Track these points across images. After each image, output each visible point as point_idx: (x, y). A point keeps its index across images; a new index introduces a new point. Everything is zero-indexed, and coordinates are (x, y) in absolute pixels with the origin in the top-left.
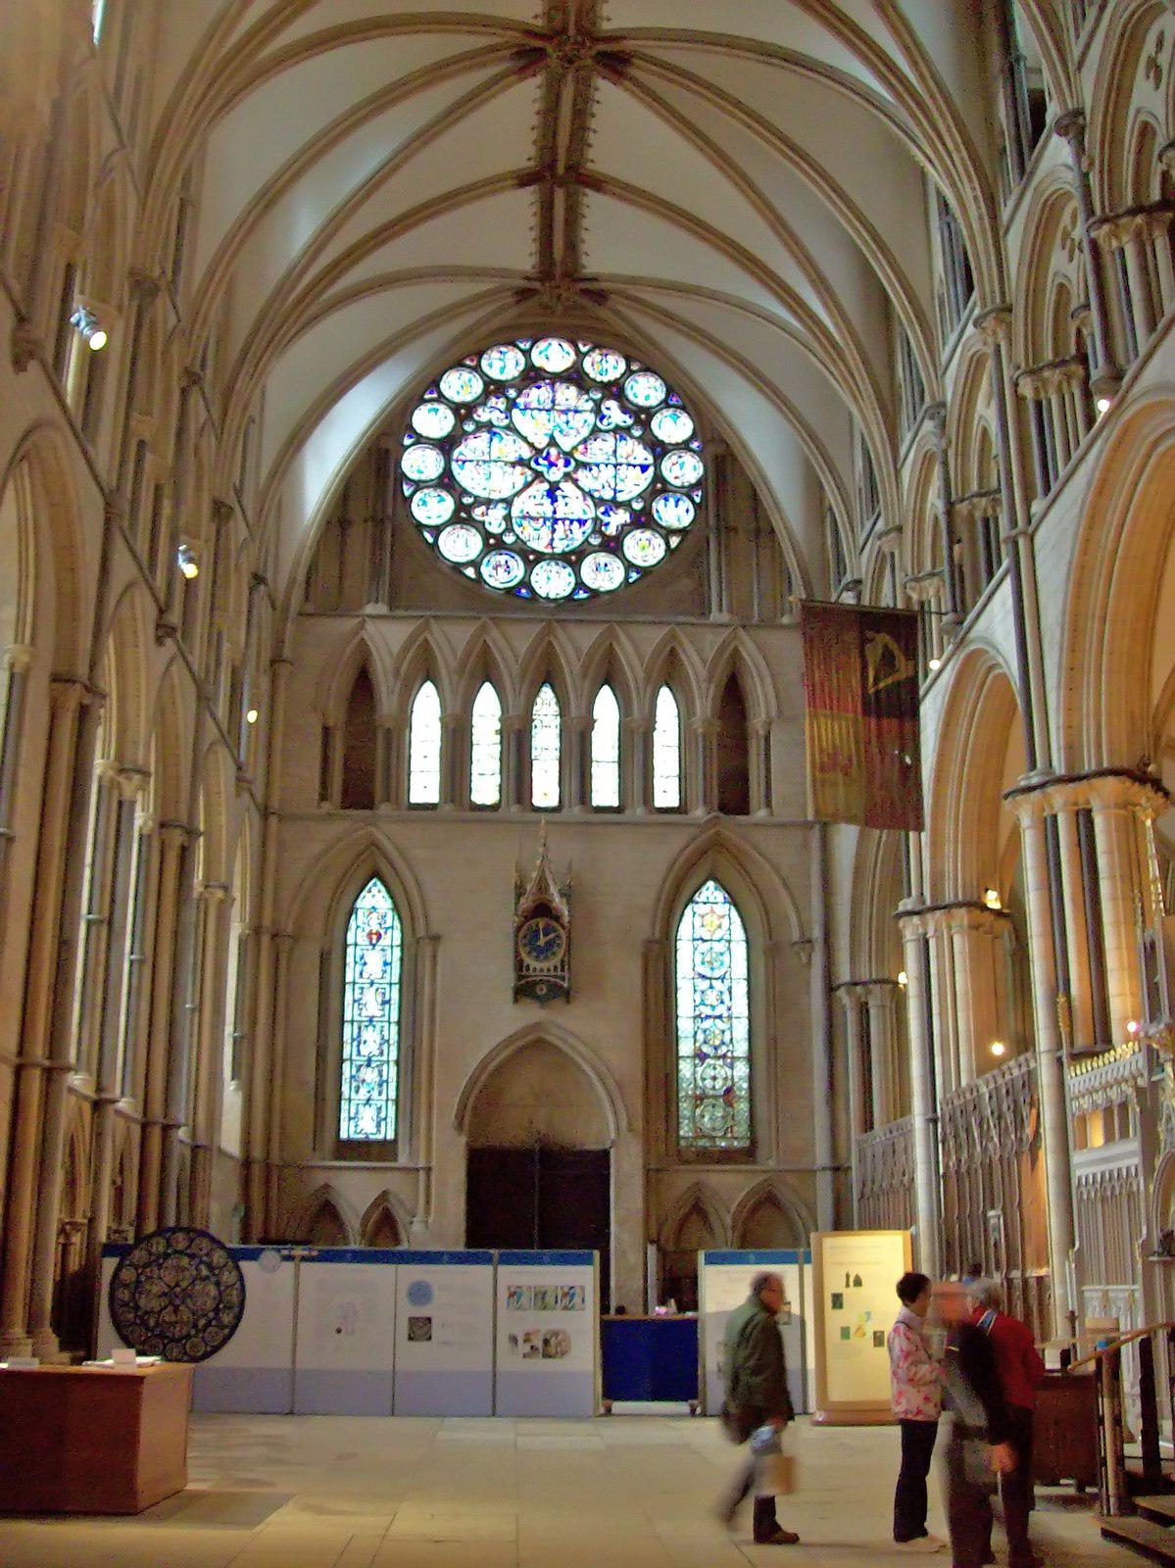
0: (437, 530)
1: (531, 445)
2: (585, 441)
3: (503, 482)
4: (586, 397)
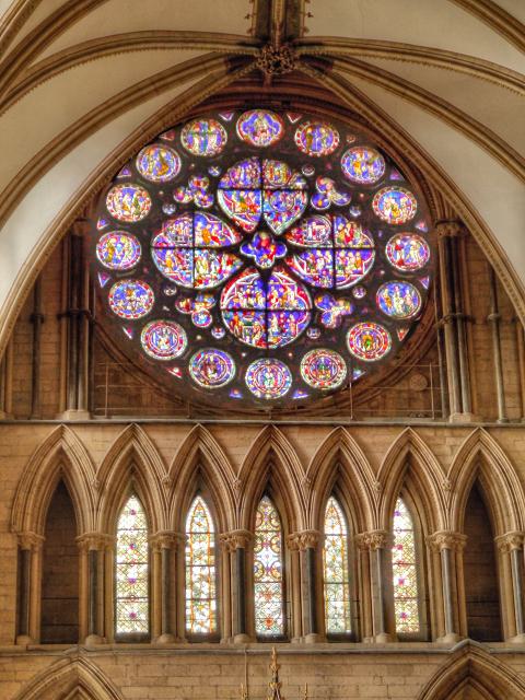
0: (137, 326)
1: (239, 230)
2: (297, 224)
3: (209, 270)
4: (298, 175)
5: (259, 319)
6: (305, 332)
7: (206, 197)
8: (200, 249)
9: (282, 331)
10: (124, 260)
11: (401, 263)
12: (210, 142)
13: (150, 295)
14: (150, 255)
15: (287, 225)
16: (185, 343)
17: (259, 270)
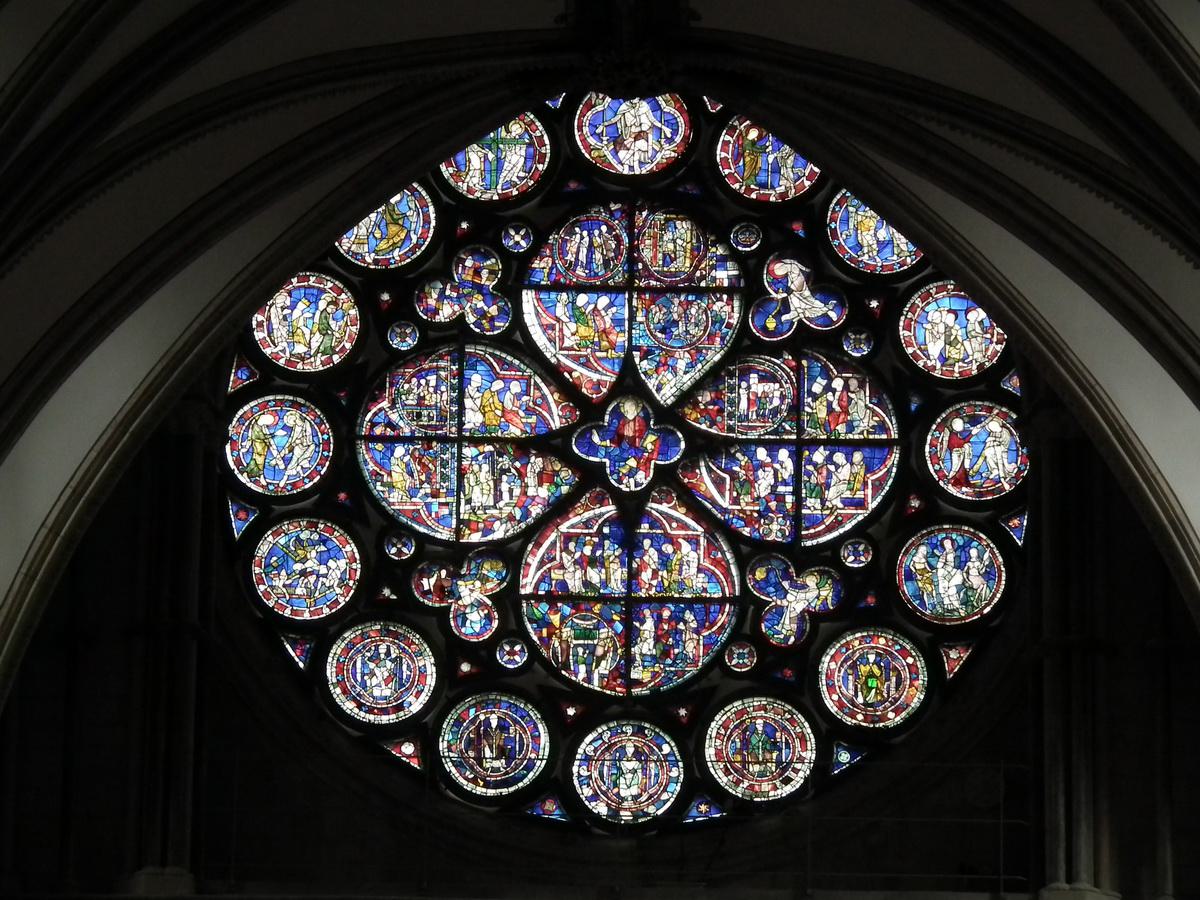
0: (321, 635)
1: (569, 391)
2: (713, 378)
4: (720, 251)
5: (611, 622)
7: (493, 310)
8: (475, 441)
9: (666, 653)
10: (292, 471)
11: (962, 479)
14: (354, 453)
15: (687, 381)
16: (431, 681)
17: (619, 497)
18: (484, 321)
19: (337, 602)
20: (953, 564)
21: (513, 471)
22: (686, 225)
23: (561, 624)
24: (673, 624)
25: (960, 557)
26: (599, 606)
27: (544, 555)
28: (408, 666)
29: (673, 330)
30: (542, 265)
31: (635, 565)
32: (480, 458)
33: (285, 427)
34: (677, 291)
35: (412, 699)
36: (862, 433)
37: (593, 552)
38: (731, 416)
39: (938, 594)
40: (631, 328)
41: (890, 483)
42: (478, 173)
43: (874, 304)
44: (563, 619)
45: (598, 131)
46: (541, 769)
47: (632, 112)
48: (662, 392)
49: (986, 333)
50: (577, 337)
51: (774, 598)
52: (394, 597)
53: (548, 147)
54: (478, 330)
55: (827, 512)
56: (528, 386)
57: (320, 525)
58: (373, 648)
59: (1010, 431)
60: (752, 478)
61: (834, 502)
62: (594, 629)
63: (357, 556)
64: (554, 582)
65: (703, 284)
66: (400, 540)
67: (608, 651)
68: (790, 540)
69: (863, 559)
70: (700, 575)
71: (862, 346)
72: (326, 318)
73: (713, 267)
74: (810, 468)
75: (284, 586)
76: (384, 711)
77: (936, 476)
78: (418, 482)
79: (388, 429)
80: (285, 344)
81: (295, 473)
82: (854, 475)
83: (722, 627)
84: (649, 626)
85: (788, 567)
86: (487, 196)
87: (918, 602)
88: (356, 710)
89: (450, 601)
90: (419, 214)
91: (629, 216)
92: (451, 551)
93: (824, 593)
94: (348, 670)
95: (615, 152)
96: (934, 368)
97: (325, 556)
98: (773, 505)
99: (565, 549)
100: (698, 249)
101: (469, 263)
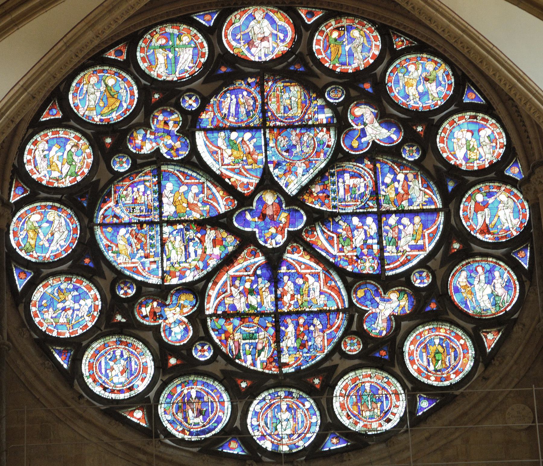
2: (321, 175)
4: (320, 102)
5: (266, 328)
6: (338, 344)
7: (178, 145)
8: (171, 223)
9: (303, 345)
10: (53, 247)
11: (485, 230)
12: (181, 60)
13: (96, 299)
15: (305, 180)
16: (151, 371)
17: (265, 251)
18: (172, 152)
19: (86, 326)
20: (484, 282)
21: (197, 239)
22: (297, 88)
23: (234, 330)
24: (307, 327)
25: (488, 277)
26: (257, 318)
27: (219, 290)
28: (136, 363)
29: (293, 150)
30: (207, 116)
31: (279, 292)
32: (175, 233)
33: (48, 222)
34: (294, 127)
35: (139, 382)
36: (419, 205)
37: (251, 286)
38: (334, 199)
39: (476, 300)
40: (266, 151)
41: (439, 234)
42: (163, 65)
43: (419, 129)
44: (234, 328)
45: (238, 37)
46: (226, 422)
47: (258, 26)
48: (289, 187)
49: (492, 142)
50: (232, 158)
51: (371, 308)
52: (124, 320)
53: (207, 48)
54: (168, 157)
55: (401, 254)
56: (203, 188)
57: (73, 279)
58: (112, 353)
59: (514, 200)
60: (350, 236)
61: (405, 248)
62: (255, 333)
63: (99, 297)
64: (227, 306)
65: (310, 123)
66: (125, 285)
67: (265, 346)
68: (378, 272)
69: (426, 281)
70: (322, 296)
71: (414, 154)
72: (71, 155)
73: (315, 113)
74: (387, 228)
75: (52, 318)
76: (121, 391)
77: (468, 229)
78: (135, 250)
79: (115, 219)
80: (46, 172)
81: (55, 248)
82: (415, 231)
83: (339, 327)
84: (291, 329)
85: (378, 289)
86: (169, 79)
87: (464, 305)
88: (103, 392)
89: (160, 321)
90: (127, 91)
91: (261, 85)
92: (159, 290)
93: (402, 303)
94: (96, 369)
95: (249, 49)
96: (461, 165)
97: (78, 298)
98: (365, 251)
99: (233, 285)
100: (306, 102)
101: (161, 117)
